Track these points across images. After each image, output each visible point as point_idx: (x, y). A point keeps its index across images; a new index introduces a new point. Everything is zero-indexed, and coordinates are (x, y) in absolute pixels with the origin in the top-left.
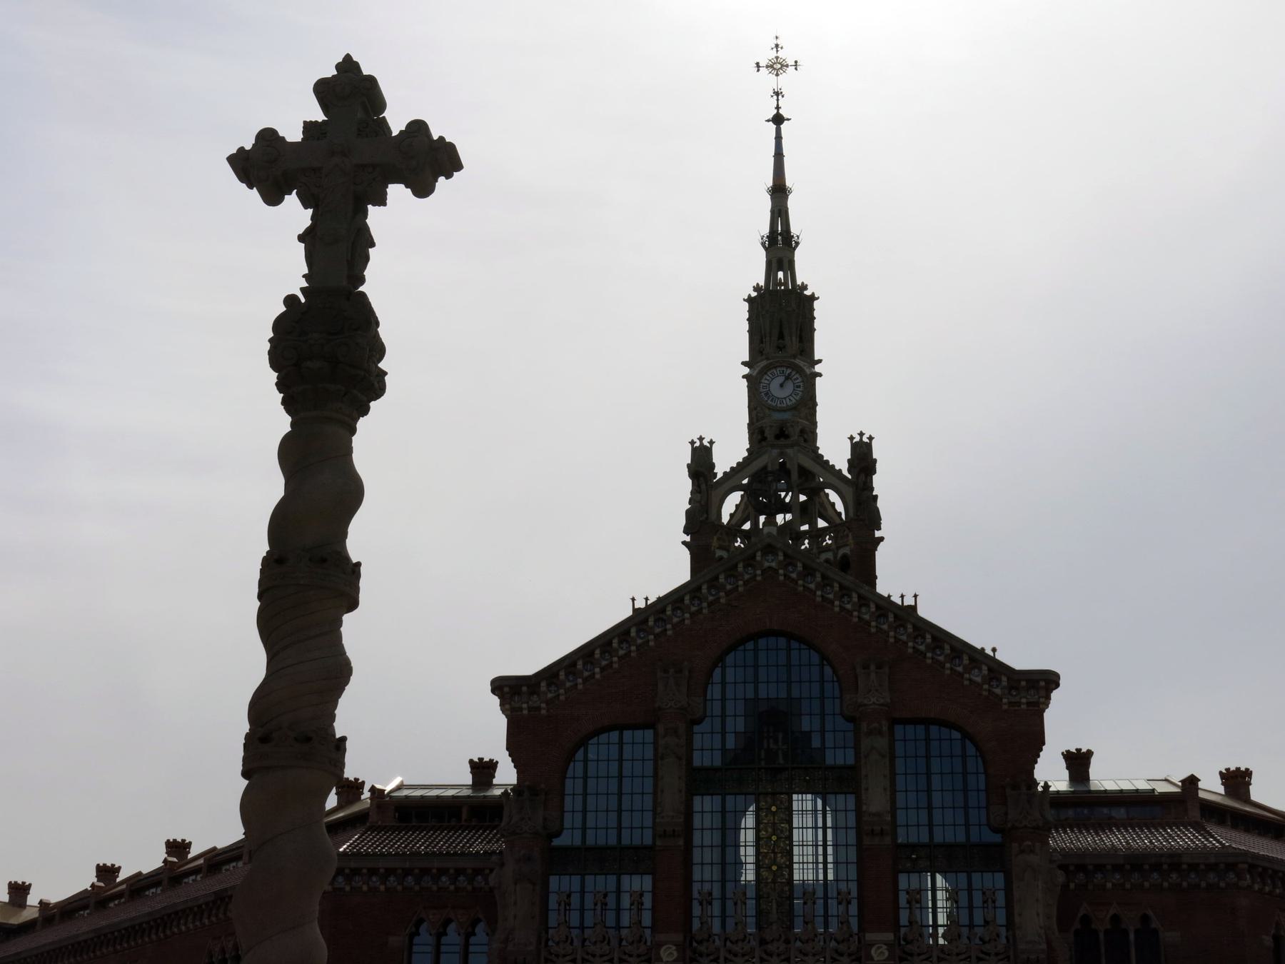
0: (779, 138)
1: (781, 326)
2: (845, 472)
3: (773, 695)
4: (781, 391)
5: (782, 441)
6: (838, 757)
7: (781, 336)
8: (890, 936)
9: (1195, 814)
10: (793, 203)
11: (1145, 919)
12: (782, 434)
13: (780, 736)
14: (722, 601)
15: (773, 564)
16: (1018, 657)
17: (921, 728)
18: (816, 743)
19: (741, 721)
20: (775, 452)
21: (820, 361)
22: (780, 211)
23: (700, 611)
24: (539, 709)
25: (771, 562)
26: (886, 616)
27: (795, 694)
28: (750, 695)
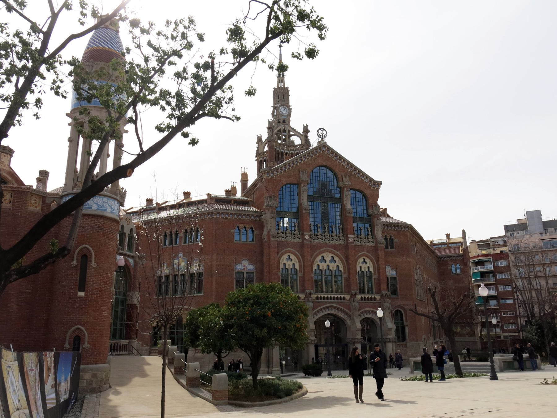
0: (280, 50)
4: (284, 112)
5: (284, 123)
6: (338, 196)
7: (284, 98)
9: (387, 216)
11: (391, 236)
12: (284, 121)
13: (325, 189)
15: (325, 150)
16: (376, 178)
17: (354, 191)
18: (333, 192)
19: (317, 185)
20: (283, 126)
23: (309, 158)
24: (273, 177)
25: (324, 149)
26: (348, 165)
27: (328, 180)
28: (319, 179)
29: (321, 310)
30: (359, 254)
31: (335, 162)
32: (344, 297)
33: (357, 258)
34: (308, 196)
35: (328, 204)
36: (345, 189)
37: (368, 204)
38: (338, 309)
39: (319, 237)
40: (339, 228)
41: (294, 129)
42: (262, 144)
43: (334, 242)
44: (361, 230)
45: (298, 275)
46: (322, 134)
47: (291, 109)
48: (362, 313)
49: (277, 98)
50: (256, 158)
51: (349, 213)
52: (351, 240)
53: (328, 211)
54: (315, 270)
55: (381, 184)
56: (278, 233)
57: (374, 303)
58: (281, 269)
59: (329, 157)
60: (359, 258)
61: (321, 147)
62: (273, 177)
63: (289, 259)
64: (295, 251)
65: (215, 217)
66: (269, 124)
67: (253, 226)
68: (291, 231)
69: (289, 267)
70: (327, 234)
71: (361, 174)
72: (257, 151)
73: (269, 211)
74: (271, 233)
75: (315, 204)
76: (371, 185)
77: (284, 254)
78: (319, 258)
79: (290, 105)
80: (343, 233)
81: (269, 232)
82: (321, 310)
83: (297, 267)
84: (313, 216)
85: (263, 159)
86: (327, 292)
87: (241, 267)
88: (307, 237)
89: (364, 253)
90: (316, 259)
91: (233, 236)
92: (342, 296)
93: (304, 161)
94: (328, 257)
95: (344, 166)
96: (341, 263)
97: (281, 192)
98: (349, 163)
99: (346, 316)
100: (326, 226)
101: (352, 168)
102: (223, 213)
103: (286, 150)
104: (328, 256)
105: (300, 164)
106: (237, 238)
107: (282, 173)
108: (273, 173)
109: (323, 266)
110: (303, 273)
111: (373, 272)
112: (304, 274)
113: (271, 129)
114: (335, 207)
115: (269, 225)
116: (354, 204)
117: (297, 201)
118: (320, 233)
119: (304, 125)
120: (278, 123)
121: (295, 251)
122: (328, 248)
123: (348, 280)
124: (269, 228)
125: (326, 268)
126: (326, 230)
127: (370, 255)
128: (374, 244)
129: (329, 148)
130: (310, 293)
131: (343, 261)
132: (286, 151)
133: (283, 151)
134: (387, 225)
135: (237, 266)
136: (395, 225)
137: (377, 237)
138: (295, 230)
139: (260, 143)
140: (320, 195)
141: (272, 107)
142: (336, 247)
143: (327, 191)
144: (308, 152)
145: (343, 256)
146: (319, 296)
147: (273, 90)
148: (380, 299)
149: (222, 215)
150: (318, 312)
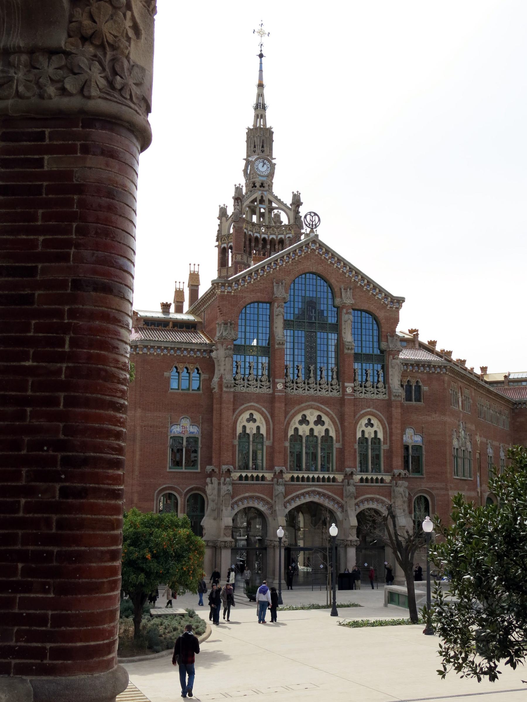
0: (261, 64)
1: (263, 143)
2: (289, 205)
3: (311, 295)
4: (262, 169)
6: (332, 320)
7: (263, 147)
8: (352, 385)
9: (417, 346)
10: (266, 91)
11: (417, 382)
12: (262, 185)
13: (313, 311)
14: (296, 259)
15: (314, 248)
16: (395, 293)
17: (359, 312)
18: (325, 315)
21: (275, 159)
22: (260, 95)
23: (288, 262)
24: (231, 292)
26: (351, 271)
27: (319, 296)
28: (303, 295)
29: (298, 496)
30: (362, 412)
31: (330, 266)
32: (334, 478)
33: (359, 417)
34: (285, 320)
35: (316, 334)
36: (344, 311)
37: (380, 333)
38: (324, 495)
39: (299, 385)
40: (332, 371)
41: (279, 198)
42: (227, 220)
43: (324, 393)
44: (367, 374)
45: (265, 443)
46: (313, 222)
47: (275, 164)
48: (362, 502)
49: (253, 146)
50: (217, 243)
51: (348, 349)
52: (349, 391)
53: (316, 345)
54: (292, 435)
55: (404, 301)
56: (235, 379)
57: (380, 486)
59: (321, 259)
60: (361, 418)
61: (308, 244)
62: (231, 292)
63: (251, 419)
64: (260, 407)
65: (141, 353)
66: (236, 192)
67: (198, 367)
68: (257, 375)
69: (251, 431)
70: (312, 380)
71: (372, 286)
72: (218, 231)
73: (222, 345)
74: (224, 380)
75: (296, 334)
76: (386, 302)
77: (244, 412)
78: (299, 417)
79: (274, 157)
80: (337, 379)
81: (221, 378)
82: (298, 496)
83: (263, 431)
84: (292, 353)
85: (227, 245)
86: (308, 469)
87: (178, 430)
88: (280, 386)
89: (369, 410)
91: (168, 381)
92: (331, 476)
93: (280, 266)
94: (312, 416)
95: (345, 273)
96: (333, 426)
97: (244, 315)
98: (352, 269)
99: (336, 506)
100: (312, 368)
101: (357, 276)
102: (153, 347)
103: (263, 233)
104: (312, 414)
105: (275, 271)
106: (174, 385)
107: (246, 286)
108: (231, 287)
109: (304, 430)
110: (271, 441)
111: (382, 439)
112: (273, 443)
113: (239, 201)
114: (328, 339)
115: (222, 368)
116: (358, 332)
117: (268, 329)
118: (302, 377)
119: (293, 193)
120: (253, 187)
121: (260, 407)
122: (313, 403)
123: (341, 451)
124: (222, 371)
126: (312, 375)
127: (380, 414)
128: (387, 397)
129: (322, 246)
130: (281, 472)
131: (336, 423)
132: (263, 236)
133: (258, 235)
134: (412, 365)
135: (173, 427)
136: (424, 365)
137: (391, 386)
138: (263, 375)
139: (224, 219)
140: (304, 319)
141: (244, 159)
142: (325, 401)
143: (315, 313)
144: (287, 253)
145: (336, 415)
146: (295, 476)
147: (247, 131)
148: (391, 481)
149: (152, 349)
150: (293, 499)
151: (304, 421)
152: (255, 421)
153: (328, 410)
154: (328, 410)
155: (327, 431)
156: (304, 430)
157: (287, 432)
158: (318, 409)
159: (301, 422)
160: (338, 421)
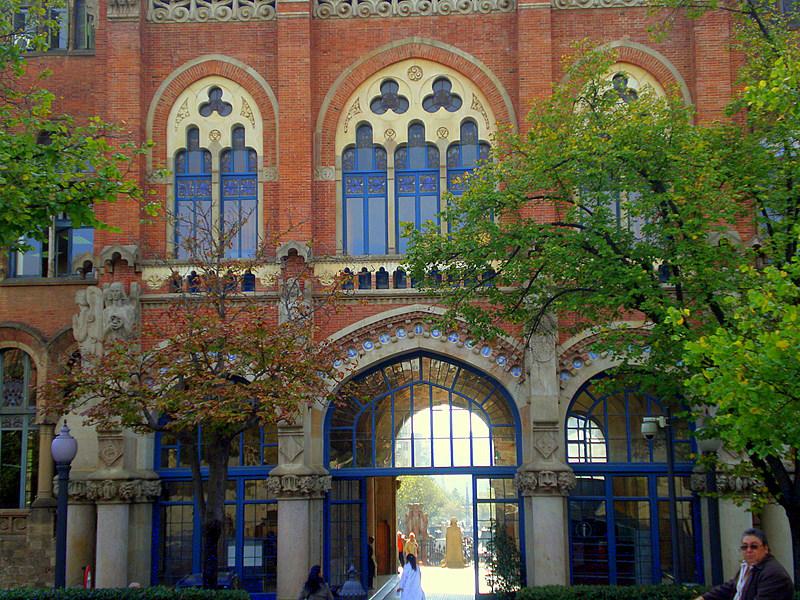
58: (171, 154)
63: (215, 104)
64: (241, 65)
78: (372, 89)
83: (254, 139)
90: (353, 99)
96: (488, 110)
109: (389, 128)
121: (241, 65)
125: (402, 136)
145: (496, 72)
151: (391, 99)
152: (225, 109)
153: (469, 57)
154: (469, 57)
155: (468, 124)
156: (389, 128)
157: (333, 138)
158: (433, 59)
159: (381, 104)
160: (502, 90)
